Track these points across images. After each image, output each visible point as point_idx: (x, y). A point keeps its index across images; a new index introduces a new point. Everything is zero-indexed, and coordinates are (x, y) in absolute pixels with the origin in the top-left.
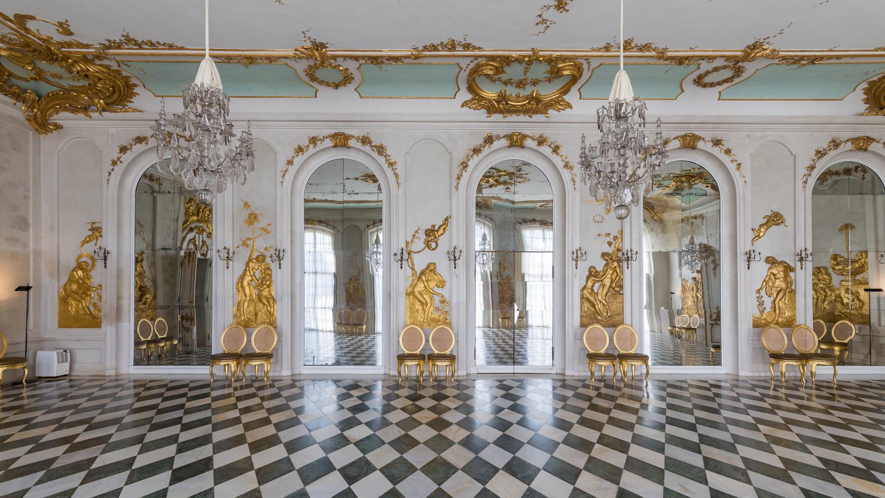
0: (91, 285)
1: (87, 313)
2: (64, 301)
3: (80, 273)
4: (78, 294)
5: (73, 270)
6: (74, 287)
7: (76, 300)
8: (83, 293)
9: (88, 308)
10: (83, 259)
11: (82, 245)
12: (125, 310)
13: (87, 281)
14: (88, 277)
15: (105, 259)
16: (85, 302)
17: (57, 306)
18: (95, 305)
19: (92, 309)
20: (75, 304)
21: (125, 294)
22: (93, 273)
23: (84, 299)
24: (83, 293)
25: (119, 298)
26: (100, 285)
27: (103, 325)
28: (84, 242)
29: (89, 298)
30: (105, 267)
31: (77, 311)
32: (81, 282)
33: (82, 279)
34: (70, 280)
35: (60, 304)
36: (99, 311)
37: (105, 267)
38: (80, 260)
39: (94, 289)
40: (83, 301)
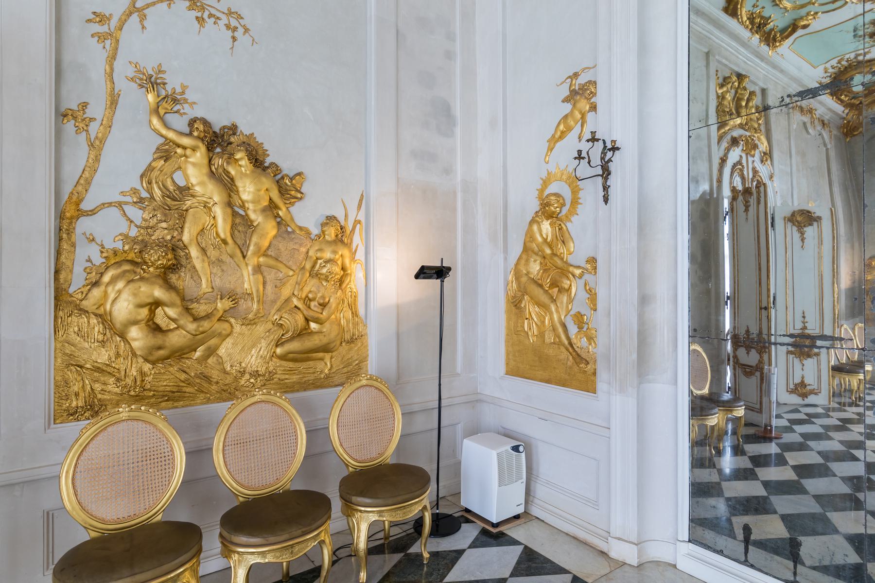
0: (571, 259)
1: (561, 343)
2: (515, 304)
3: (546, 226)
4: (541, 286)
5: (533, 221)
6: (535, 268)
7: (539, 304)
8: (554, 284)
9: (564, 326)
10: (552, 188)
11: (551, 149)
12: (661, 340)
13: (561, 249)
14: (562, 237)
15: (606, 173)
16: (557, 311)
17: (503, 317)
18: (579, 319)
19: (573, 330)
20: (537, 314)
21: (660, 289)
22: (573, 226)
23: (554, 301)
24: (554, 284)
25: (644, 300)
26: (593, 261)
27: (601, 386)
28: (554, 140)
29: (565, 299)
30: (606, 200)
31: (541, 335)
32: (548, 251)
33: (550, 246)
34: (526, 249)
35: (508, 312)
36: (590, 339)
37: (606, 200)
38: (546, 193)
39: (578, 272)
40: (553, 308)
